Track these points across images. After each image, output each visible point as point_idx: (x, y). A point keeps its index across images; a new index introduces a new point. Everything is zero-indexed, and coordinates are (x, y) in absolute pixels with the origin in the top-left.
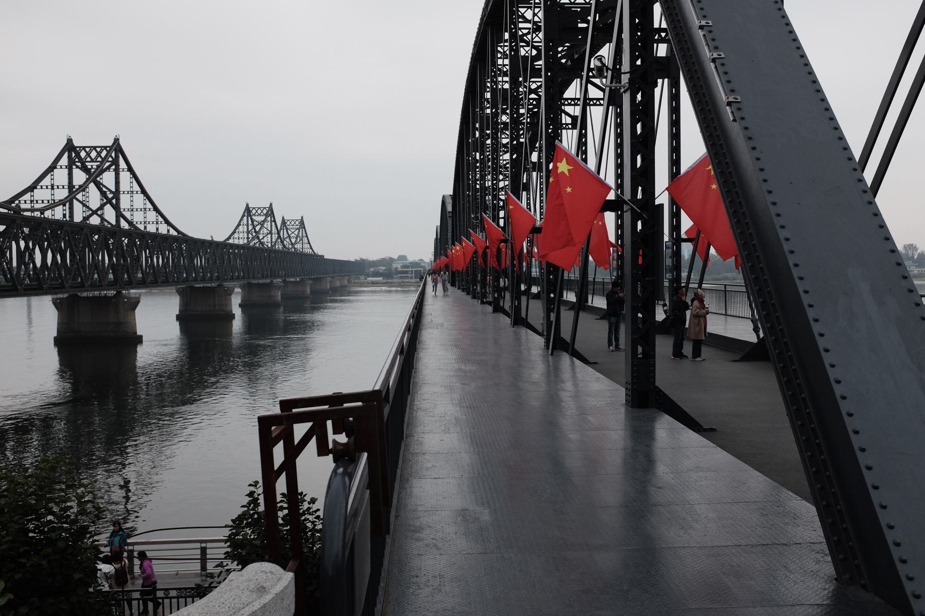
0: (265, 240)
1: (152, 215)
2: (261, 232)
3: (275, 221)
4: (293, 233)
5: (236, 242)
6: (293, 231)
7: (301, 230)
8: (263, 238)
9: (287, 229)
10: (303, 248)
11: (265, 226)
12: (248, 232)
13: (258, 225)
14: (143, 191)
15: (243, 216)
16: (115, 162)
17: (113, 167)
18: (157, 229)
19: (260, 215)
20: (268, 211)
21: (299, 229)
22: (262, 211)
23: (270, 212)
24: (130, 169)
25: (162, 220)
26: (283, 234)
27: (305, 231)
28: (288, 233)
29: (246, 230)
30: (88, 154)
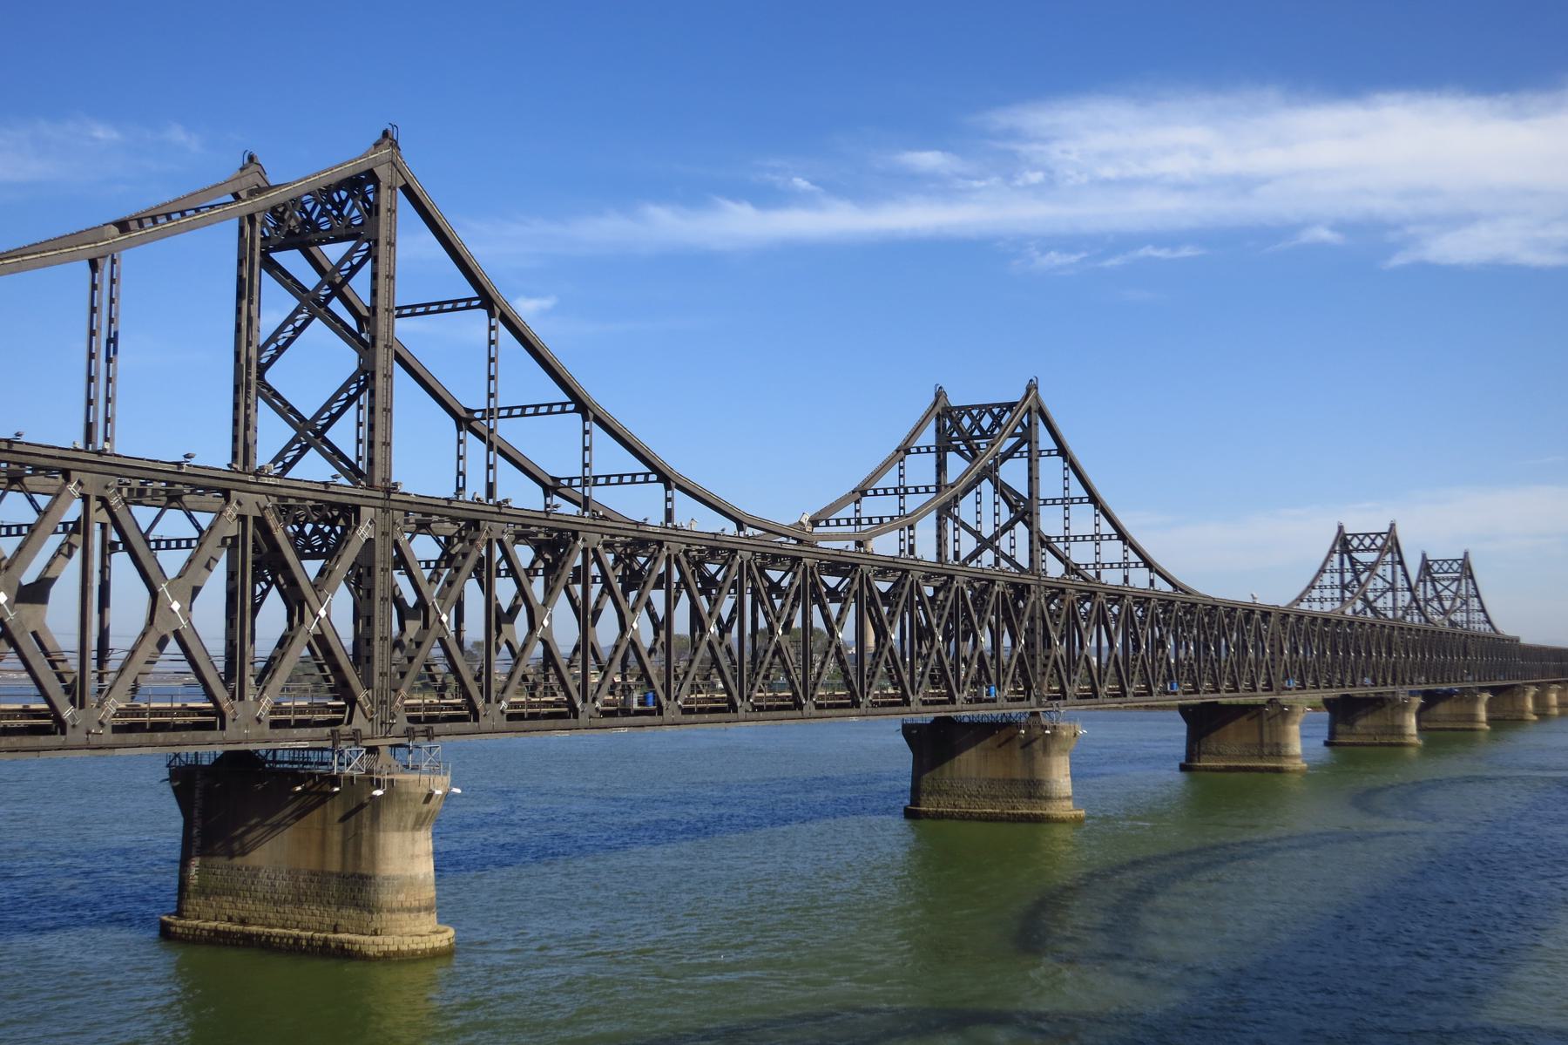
1: (1113, 550)
14: (1093, 499)
16: (1027, 437)
17: (1025, 448)
18: (1126, 579)
24: (1062, 451)
25: (1138, 559)
30: (976, 422)
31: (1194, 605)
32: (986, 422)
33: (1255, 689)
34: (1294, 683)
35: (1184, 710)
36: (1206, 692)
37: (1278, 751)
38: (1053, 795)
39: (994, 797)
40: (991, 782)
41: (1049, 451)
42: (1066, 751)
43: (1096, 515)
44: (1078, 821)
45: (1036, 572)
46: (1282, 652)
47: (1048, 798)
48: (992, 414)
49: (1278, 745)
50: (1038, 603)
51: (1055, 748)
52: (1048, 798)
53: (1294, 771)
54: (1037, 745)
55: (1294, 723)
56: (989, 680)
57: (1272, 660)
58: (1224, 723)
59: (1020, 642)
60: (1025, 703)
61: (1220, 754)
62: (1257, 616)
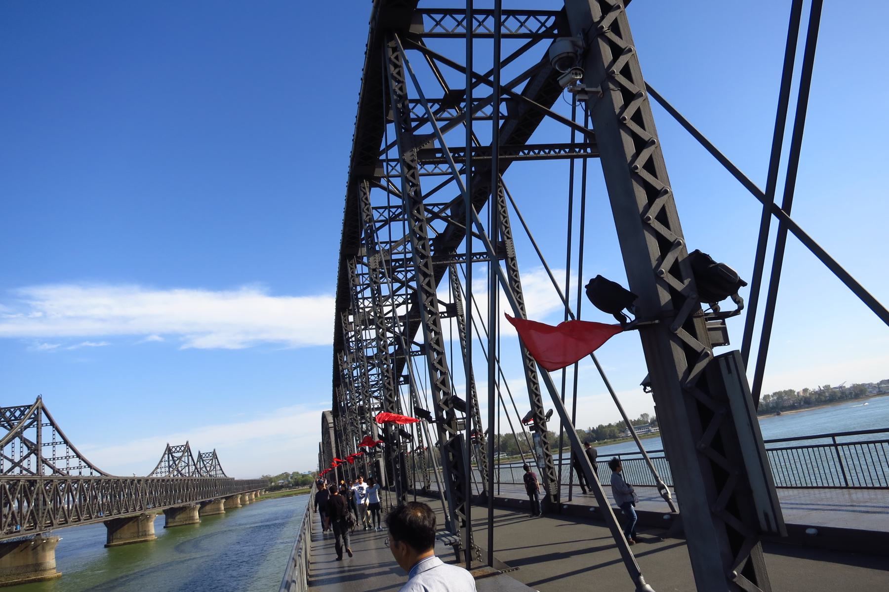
0: (183, 472)
1: (75, 462)
2: (180, 465)
3: (191, 455)
4: (208, 463)
5: (159, 475)
6: (207, 461)
7: (214, 460)
8: (182, 470)
9: (203, 461)
10: (216, 475)
11: (183, 459)
12: (170, 467)
13: (177, 460)
14: (66, 442)
15: (165, 454)
16: (36, 419)
17: (35, 423)
19: (178, 452)
20: (185, 448)
21: (212, 459)
22: (180, 449)
23: (187, 449)
24: (52, 424)
25: (86, 465)
26: (200, 465)
27: (218, 460)
28: (204, 463)
29: (167, 465)
30: (13, 414)
31: (110, 480)
32: (18, 413)
33: (135, 510)
34: (151, 506)
35: (106, 523)
36: (115, 515)
37: (145, 533)
38: (47, 568)
39: (18, 574)
40: (17, 568)
41: (47, 424)
42: (53, 548)
43: (67, 448)
44: (59, 578)
45: (40, 474)
46: (146, 495)
47: (45, 570)
48: (20, 410)
49: (145, 531)
50: (40, 489)
51: (48, 548)
52: (45, 570)
53: (152, 540)
54: (39, 548)
55: (151, 521)
56: (16, 523)
57: (142, 498)
58: (123, 525)
59: (32, 505)
60: (33, 531)
61: (121, 538)
62: (136, 482)
